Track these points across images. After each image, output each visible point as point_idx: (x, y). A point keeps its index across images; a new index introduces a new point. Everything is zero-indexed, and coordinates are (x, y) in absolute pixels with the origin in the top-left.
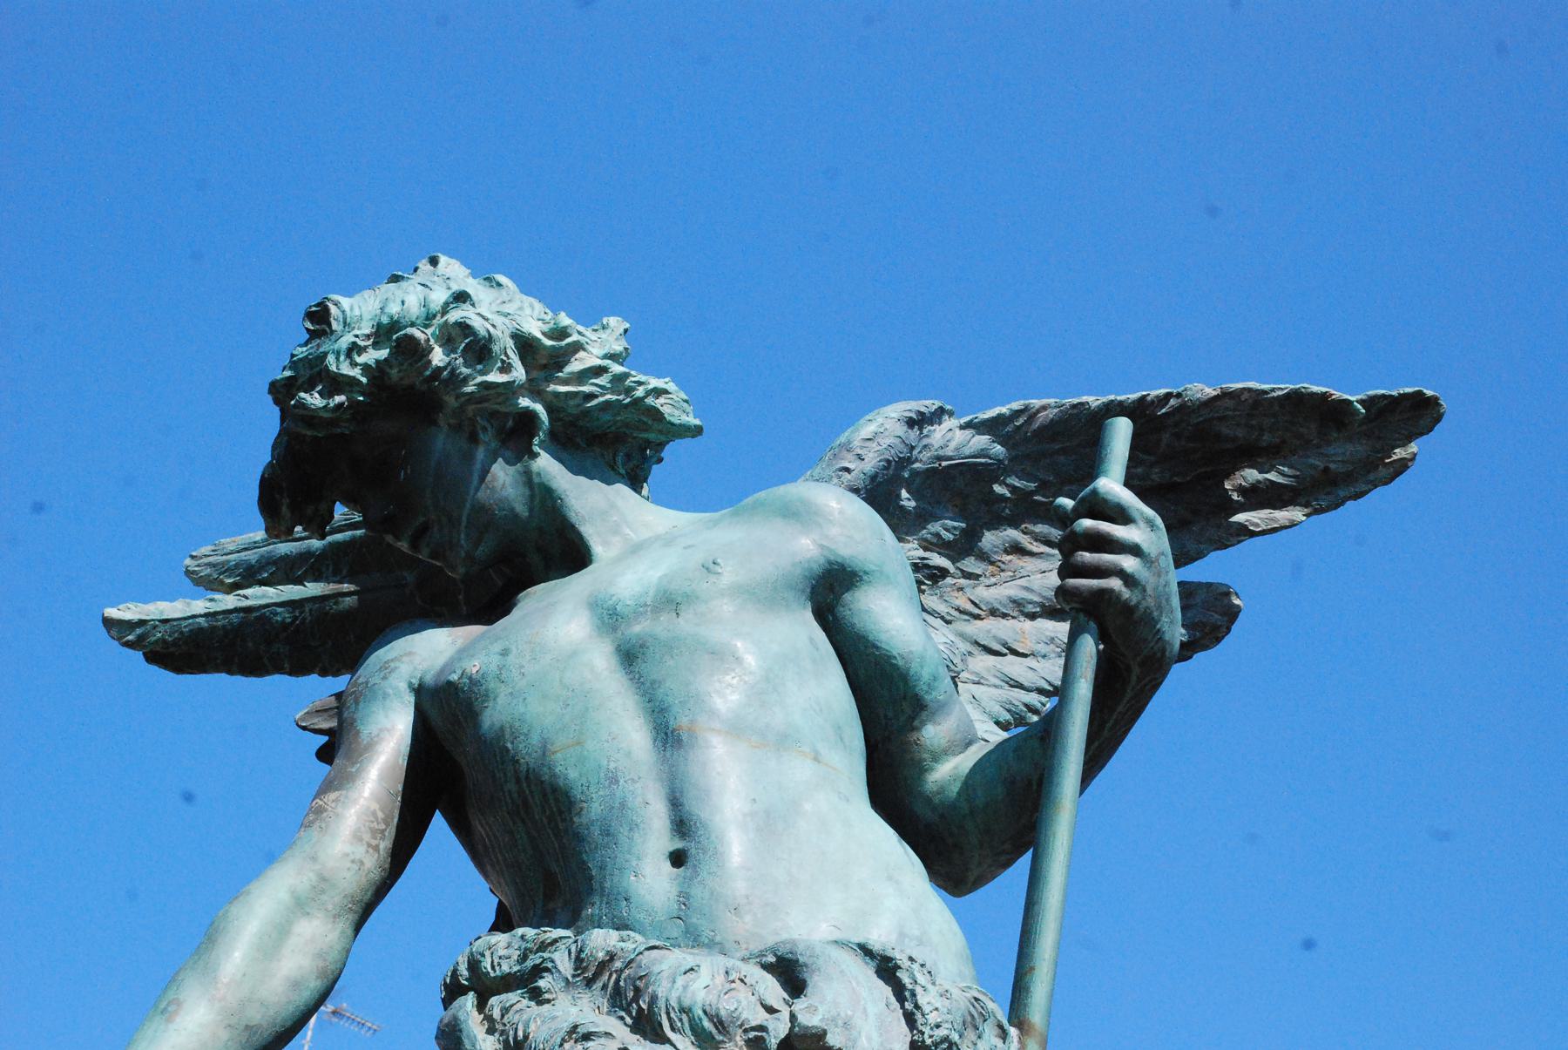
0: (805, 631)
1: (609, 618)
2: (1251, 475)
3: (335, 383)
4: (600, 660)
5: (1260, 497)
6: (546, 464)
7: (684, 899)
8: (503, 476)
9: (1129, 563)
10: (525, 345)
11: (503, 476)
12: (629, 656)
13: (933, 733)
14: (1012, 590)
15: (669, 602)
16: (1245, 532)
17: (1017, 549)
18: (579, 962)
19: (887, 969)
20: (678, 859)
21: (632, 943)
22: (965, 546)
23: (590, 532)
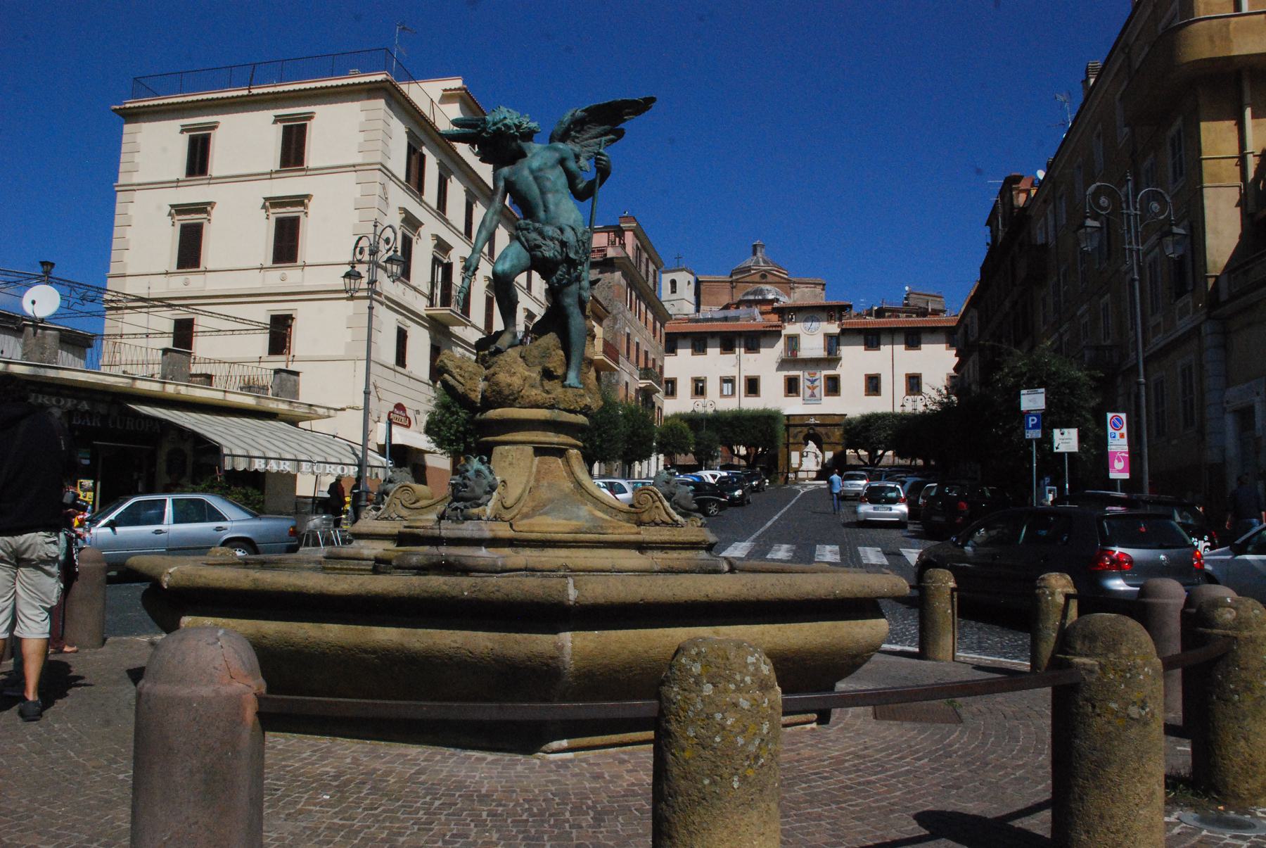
0: (560, 169)
1: (532, 171)
2: (627, 110)
3: (487, 133)
4: (531, 178)
5: (628, 114)
6: (519, 141)
7: (547, 218)
8: (514, 145)
9: (604, 163)
10: (515, 125)
11: (514, 145)
12: (536, 178)
13: (578, 181)
14: (588, 136)
15: (540, 169)
16: (625, 120)
17: (590, 128)
18: (534, 228)
19: (573, 229)
20: (545, 211)
21: (541, 226)
22: (582, 129)
23: (527, 152)
